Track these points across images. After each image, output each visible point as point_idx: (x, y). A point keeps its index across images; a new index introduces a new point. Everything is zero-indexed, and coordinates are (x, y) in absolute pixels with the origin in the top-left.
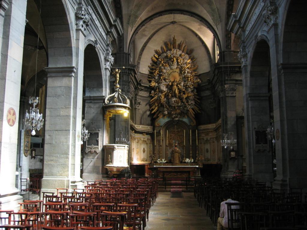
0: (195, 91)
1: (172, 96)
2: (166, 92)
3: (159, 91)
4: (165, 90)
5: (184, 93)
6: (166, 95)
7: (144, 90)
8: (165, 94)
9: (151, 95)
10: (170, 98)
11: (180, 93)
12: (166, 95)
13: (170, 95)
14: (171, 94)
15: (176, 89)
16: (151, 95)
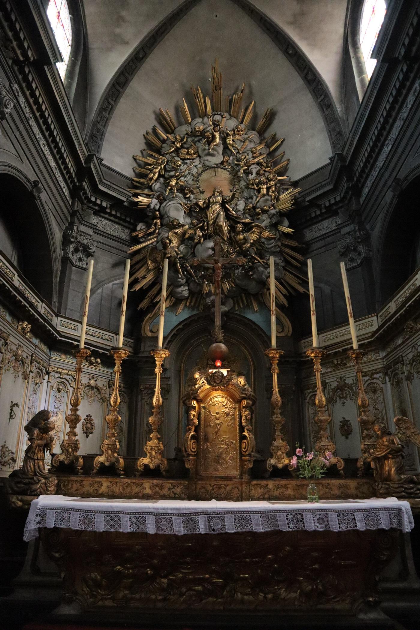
0: (286, 222)
1: (207, 237)
2: (187, 226)
3: (162, 225)
4: (182, 221)
5: (248, 228)
6: (187, 236)
7: (110, 214)
8: (184, 233)
9: (134, 234)
10: (199, 242)
11: (232, 229)
12: (187, 236)
13: (201, 234)
14: (202, 228)
15: (219, 214)
16: (134, 234)
